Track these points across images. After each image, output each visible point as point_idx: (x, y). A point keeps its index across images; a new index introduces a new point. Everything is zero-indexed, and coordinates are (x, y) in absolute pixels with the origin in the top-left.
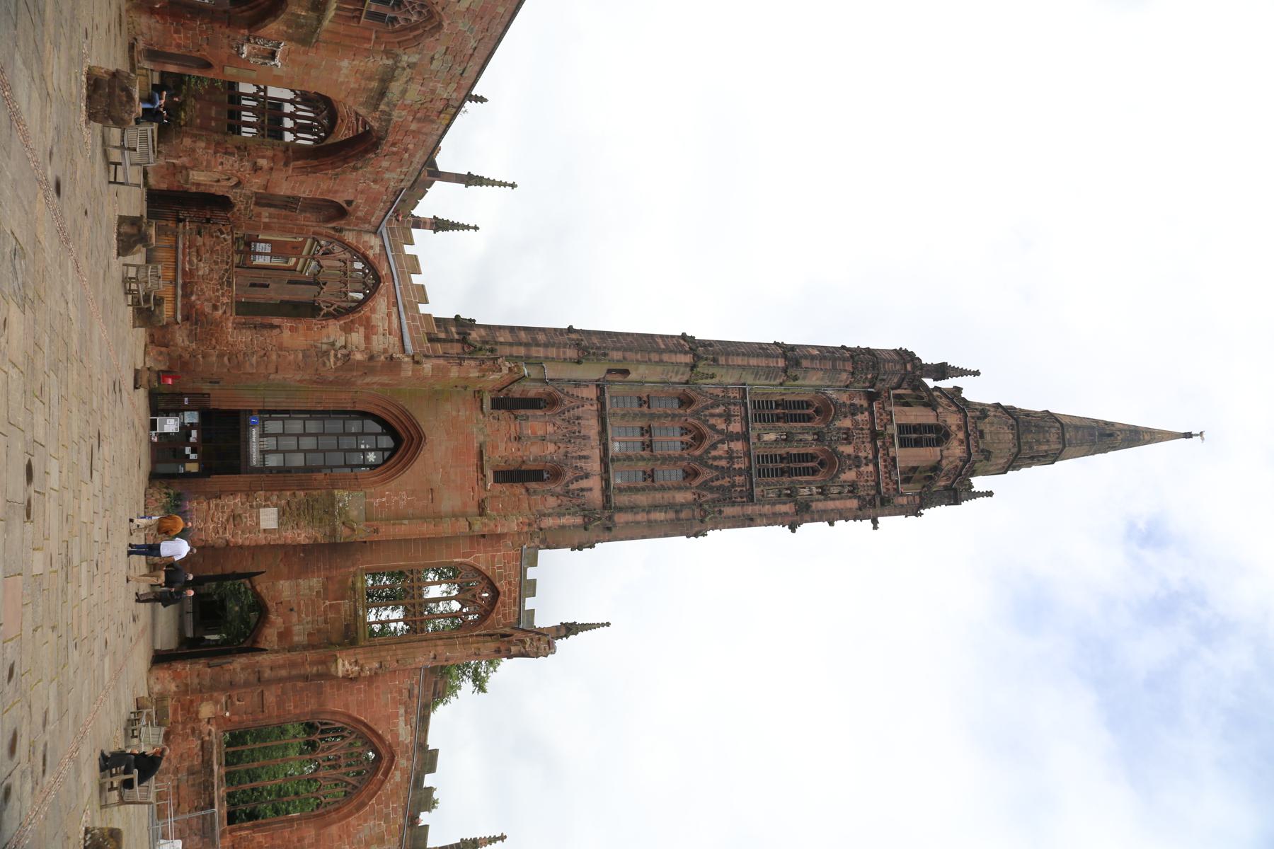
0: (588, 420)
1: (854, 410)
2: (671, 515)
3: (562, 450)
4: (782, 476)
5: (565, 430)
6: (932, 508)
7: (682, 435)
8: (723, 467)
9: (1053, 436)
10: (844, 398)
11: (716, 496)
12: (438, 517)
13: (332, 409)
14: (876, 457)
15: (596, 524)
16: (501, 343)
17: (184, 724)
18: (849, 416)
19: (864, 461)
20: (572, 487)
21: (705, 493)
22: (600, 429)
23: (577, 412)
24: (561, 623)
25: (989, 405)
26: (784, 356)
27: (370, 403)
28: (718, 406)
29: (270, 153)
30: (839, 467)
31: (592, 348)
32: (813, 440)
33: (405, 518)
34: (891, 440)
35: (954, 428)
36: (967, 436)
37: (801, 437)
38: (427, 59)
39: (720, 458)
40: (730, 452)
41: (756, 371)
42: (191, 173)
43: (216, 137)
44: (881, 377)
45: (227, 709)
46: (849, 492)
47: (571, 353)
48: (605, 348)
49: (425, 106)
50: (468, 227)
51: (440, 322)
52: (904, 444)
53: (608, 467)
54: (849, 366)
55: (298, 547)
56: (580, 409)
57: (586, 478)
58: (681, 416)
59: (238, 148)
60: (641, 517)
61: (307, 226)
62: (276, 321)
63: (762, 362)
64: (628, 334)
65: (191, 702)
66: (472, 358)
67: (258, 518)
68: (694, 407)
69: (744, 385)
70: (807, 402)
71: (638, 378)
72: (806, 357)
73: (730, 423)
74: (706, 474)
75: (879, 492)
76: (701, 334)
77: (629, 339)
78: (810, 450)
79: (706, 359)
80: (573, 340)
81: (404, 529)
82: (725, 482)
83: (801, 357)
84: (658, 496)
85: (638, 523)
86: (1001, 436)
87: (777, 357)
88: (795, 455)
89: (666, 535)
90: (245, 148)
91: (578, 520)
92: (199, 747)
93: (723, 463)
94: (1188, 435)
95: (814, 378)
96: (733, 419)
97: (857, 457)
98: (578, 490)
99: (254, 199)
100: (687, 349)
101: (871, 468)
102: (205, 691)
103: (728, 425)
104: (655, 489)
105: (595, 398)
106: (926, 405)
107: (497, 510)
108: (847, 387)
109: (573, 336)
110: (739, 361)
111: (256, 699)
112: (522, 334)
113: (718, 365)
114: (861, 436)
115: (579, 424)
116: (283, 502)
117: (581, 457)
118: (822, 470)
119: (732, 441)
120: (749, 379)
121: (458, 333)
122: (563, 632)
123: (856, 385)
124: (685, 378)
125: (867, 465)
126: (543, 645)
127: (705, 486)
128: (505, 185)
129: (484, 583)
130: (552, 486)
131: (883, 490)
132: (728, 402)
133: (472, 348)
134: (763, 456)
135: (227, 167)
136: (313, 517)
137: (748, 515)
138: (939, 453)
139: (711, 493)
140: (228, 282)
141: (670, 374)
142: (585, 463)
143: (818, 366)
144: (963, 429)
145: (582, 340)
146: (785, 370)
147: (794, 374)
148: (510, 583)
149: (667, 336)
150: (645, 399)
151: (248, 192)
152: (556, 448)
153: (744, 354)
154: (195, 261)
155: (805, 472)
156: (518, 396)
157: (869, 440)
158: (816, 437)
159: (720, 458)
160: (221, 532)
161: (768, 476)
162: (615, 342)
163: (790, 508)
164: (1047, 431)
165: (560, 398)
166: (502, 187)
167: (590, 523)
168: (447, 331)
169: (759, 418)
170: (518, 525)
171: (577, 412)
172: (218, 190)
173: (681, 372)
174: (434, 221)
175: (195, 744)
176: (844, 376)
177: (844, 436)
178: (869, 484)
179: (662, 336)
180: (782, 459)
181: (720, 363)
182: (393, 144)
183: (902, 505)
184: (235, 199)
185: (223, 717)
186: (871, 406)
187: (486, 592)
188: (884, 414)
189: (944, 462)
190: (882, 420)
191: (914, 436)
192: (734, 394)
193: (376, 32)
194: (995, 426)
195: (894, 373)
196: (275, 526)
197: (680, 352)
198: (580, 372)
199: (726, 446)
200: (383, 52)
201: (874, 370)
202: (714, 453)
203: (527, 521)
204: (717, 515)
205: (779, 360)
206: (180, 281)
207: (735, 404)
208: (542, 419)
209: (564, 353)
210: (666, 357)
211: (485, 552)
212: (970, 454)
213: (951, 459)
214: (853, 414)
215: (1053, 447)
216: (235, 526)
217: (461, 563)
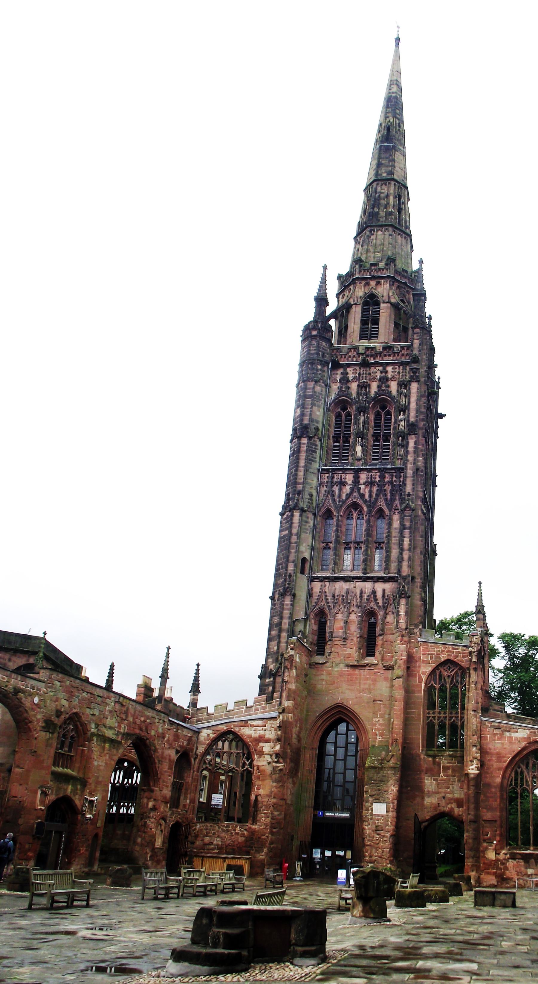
0: (335, 589)
1: (345, 380)
2: (407, 533)
3: (355, 609)
5: (341, 606)
7: (353, 518)
8: (377, 490)
9: (384, 190)
10: (335, 387)
12: (391, 698)
13: (316, 764)
15: (406, 589)
16: (278, 649)
17: (498, 868)
18: (349, 385)
20: (381, 604)
23: (329, 597)
25: (355, 248)
26: (299, 438)
27: (314, 738)
28: (333, 491)
29: (145, 800)
31: (285, 585)
32: (364, 415)
33: (390, 720)
36: (373, 278)
37: (361, 426)
39: (371, 492)
40: (366, 484)
41: (309, 461)
42: (156, 846)
43: (135, 830)
45: (492, 843)
46: (405, 388)
48: (285, 576)
52: (374, 335)
53: (369, 577)
55: (400, 791)
56: (328, 594)
59: (142, 819)
60: (406, 555)
61: (193, 776)
62: (253, 797)
63: (303, 455)
65: (484, 863)
67: (378, 815)
68: (333, 509)
69: (319, 470)
70: (337, 417)
71: (309, 551)
72: (302, 420)
73: (346, 482)
74: (382, 503)
75: (407, 363)
76: (281, 501)
78: (372, 417)
79: (298, 500)
80: (279, 597)
81: (398, 722)
82: (388, 488)
83: (301, 424)
84: (394, 540)
85: (409, 559)
86: (379, 242)
87: (300, 443)
88: (375, 430)
90: (142, 814)
91: (403, 602)
92: (513, 861)
93: (375, 489)
95: (318, 413)
96: (343, 480)
98: (383, 600)
99: (174, 809)
101: (389, 369)
102: (478, 854)
103: (347, 484)
104: (388, 543)
105: (320, 584)
106: (348, 311)
107: (392, 657)
108: (326, 386)
109: (277, 597)
110: (301, 474)
111: (488, 825)
113: (302, 490)
115: (337, 596)
116: (370, 799)
117: (361, 596)
119: (359, 482)
120: (316, 465)
123: (325, 379)
124: (311, 516)
125: (386, 372)
127: (390, 504)
130: (379, 617)
132: (332, 484)
135: (153, 825)
136: (381, 781)
137: (414, 473)
138: (385, 305)
139: (395, 500)
140: (227, 827)
141: (307, 527)
142: (365, 593)
143: (309, 410)
144: (369, 281)
145: (279, 591)
146: (310, 438)
147: (314, 430)
148: (442, 651)
151: (169, 814)
152: (353, 613)
153: (296, 470)
154: (213, 846)
156: (316, 637)
157: (368, 369)
158: (362, 414)
160: (386, 839)
162: (282, 567)
163: (412, 439)
165: (319, 608)
167: (406, 593)
168: (268, 685)
170: (402, 644)
171: (329, 597)
172: (167, 832)
175: (511, 863)
176: (318, 388)
177: (363, 389)
178: (401, 371)
181: (301, 489)
183: (420, 344)
184: (173, 821)
185: (496, 845)
186: (342, 366)
188: (350, 354)
189: (393, 300)
190: (354, 356)
192: (326, 477)
194: (370, 247)
195: (318, 347)
196: (386, 804)
197: (292, 520)
198: (302, 594)
199: (363, 487)
201: (314, 364)
203: (400, 638)
204: (410, 498)
205: (302, 442)
206: (225, 856)
207: (333, 478)
208: (333, 622)
209: (287, 605)
210: (295, 531)
211: (420, 667)
212: (388, 277)
214: (348, 381)
215: (392, 191)
216: (382, 830)
217: (426, 684)
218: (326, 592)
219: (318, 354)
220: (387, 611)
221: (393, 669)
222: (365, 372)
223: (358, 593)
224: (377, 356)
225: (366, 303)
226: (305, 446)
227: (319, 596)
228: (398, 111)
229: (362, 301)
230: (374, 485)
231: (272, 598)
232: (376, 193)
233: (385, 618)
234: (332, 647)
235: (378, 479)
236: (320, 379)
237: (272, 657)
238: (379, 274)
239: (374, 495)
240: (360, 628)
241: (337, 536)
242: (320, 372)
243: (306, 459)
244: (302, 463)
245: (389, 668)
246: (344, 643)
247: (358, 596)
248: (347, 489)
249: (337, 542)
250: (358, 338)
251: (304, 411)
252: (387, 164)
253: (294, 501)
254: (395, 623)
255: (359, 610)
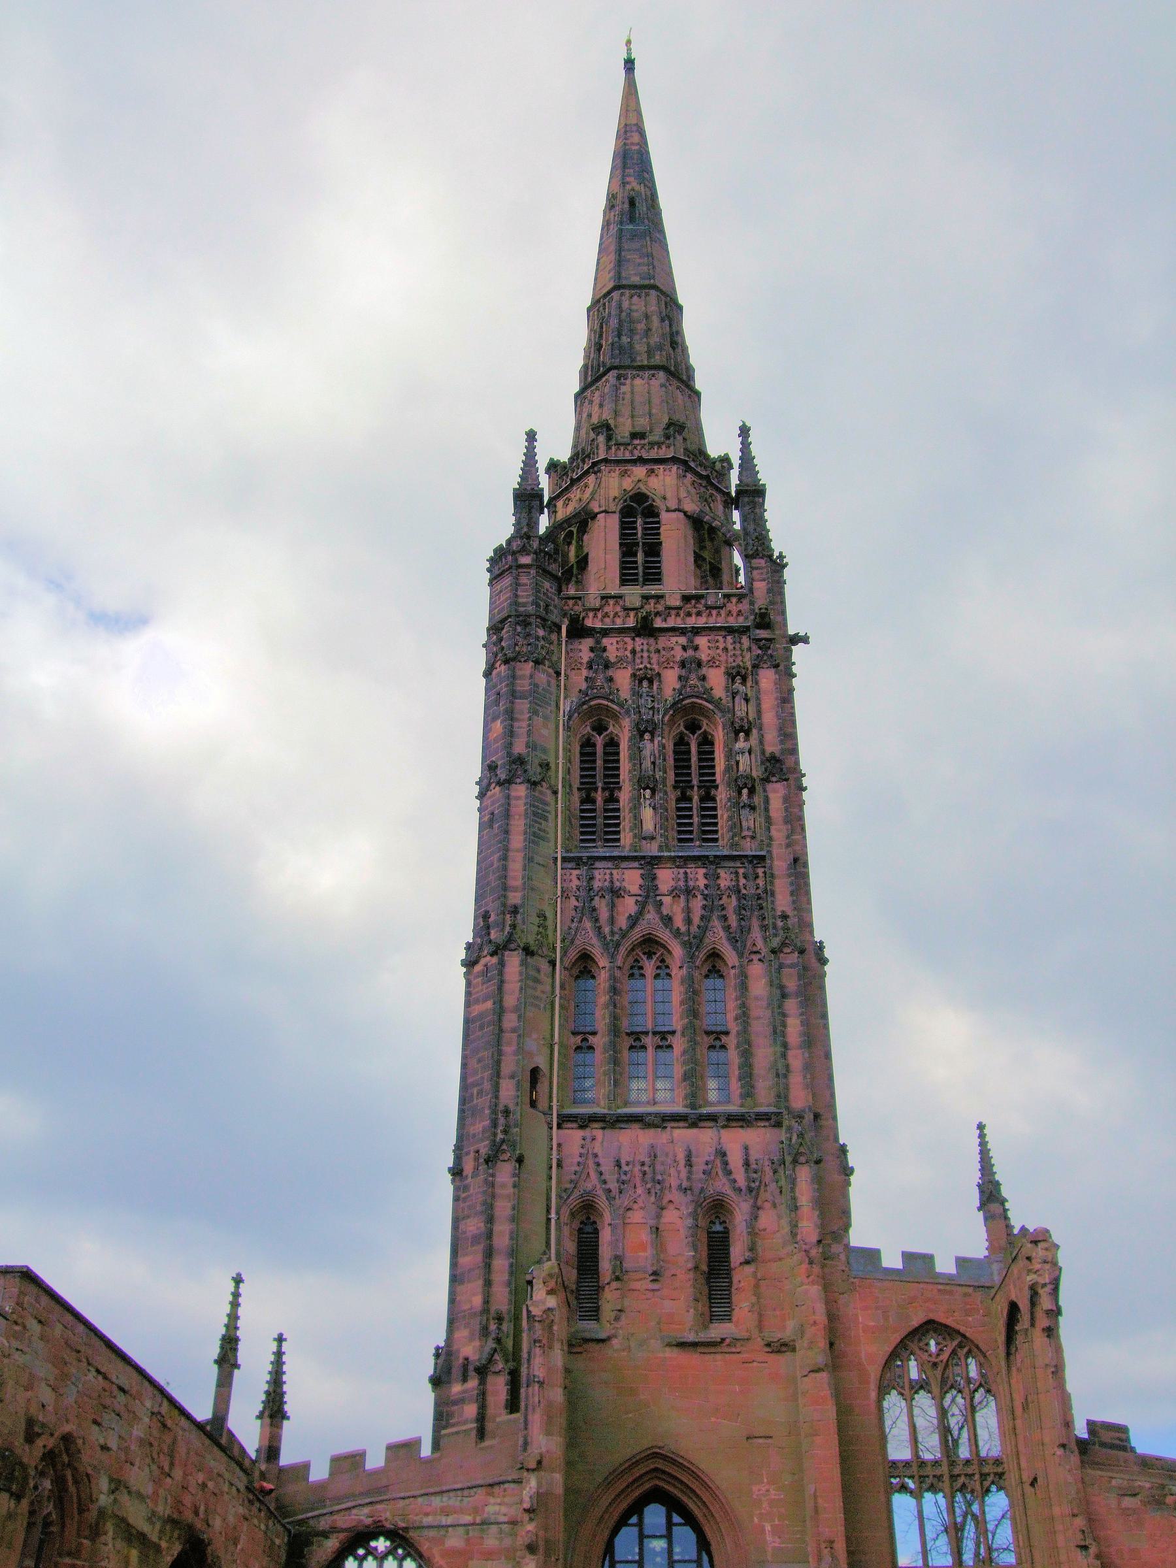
1: (601, 663)
3: (677, 1196)
4: (714, 799)
5: (639, 1191)
6: (771, 535)
8: (704, 907)
9: (638, 305)
11: (755, 924)
14: (682, 631)
16: (486, 1302)
19: (690, 652)
20: (742, 1182)
21: (749, 943)
22: (636, 1126)
23: (607, 1166)
24: (979, 1209)
28: (594, 909)
30: (702, 698)
31: (495, 1135)
34: (652, 601)
35: (628, 484)
36: (641, 461)
37: (647, 764)
38: (104, 1456)
39: (688, 910)
40: (674, 893)
41: (535, 837)
44: (542, 612)
47: (505, 1172)
49: (156, 1456)
50: (279, 1354)
51: (442, 1418)
52: (653, 575)
54: (527, 668)
56: (601, 1160)
57: (724, 1154)
58: (613, 978)
60: (796, 1060)
64: (464, 1066)
66: (529, 1360)
70: (582, 746)
74: (718, 937)
75: (744, 630)
77: (473, 1063)
79: (514, 926)
83: (509, 754)
87: (508, 797)
88: (676, 775)
89: (824, 1016)
93: (698, 903)
94: (629, 65)
95: (544, 732)
96: (617, 884)
97: (683, 664)
98: (747, 1171)
100: (495, 960)
101: (702, 641)
105: (580, 1133)
109: (468, 1166)
110: (516, 865)
112: (464, 1260)
113: (523, 905)
114: (645, 654)
117: (689, 1163)
118: (704, 727)
121: (465, 1380)
122: (994, 1207)
123: (555, 658)
125: (696, 648)
126: (1039, 1252)
128: (236, 1295)
129: (913, 1346)
131: (741, 622)
133: (496, 1357)
134: (679, 832)
138: (674, 515)
141: (538, 993)
144: (629, 467)
147: (539, 770)
149: (468, 994)
150: (579, 1038)
152: (671, 1207)
153: (505, 858)
155: (707, 756)
157: (652, 641)
158: (647, 736)
159: (688, 910)
161: (716, 824)
162: (480, 1093)
163: (775, 791)
164: (629, 315)
166: (241, 1300)
169: (611, 834)
171: (607, 1166)
173: (536, 975)
174: (268, 1420)
177: (645, 684)
179: (468, 1004)
180: (684, 798)
182: (196, 1513)
187: (927, 1344)
188: (606, 609)
191: (640, 557)
193: (60, 1555)
195: (537, 588)
199: (667, 900)
200: (93, 1540)
201: (530, 624)
202: (679, 922)
209: (503, 1186)
212: (674, 460)
213: (683, 494)
218: (596, 1156)
219: (538, 606)
220: (759, 1203)
221: (794, 1350)
222: (645, 647)
223: (681, 1157)
224: (669, 615)
225: (627, 513)
226: (521, 802)
227: (579, 1164)
228: (646, 176)
229: (619, 507)
230: (695, 896)
231: (457, 1172)
232: (621, 311)
233: (756, 1218)
234: (623, 1297)
235: (702, 882)
236: (545, 658)
237: (467, 1325)
238: (653, 454)
239: (696, 920)
240: (695, 1247)
241: (615, 1018)
242: (542, 642)
243: (525, 833)
244: (517, 841)
245: (783, 1347)
246: (656, 1286)
247: (682, 1162)
248: (629, 906)
249: (615, 1031)
250: (618, 582)
251: (512, 726)
252: (638, 261)
253: (503, 930)
254: (787, 1229)
255: (689, 1197)
